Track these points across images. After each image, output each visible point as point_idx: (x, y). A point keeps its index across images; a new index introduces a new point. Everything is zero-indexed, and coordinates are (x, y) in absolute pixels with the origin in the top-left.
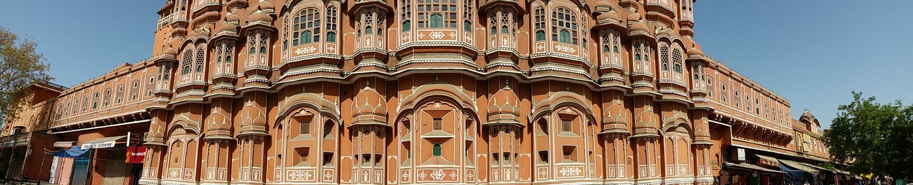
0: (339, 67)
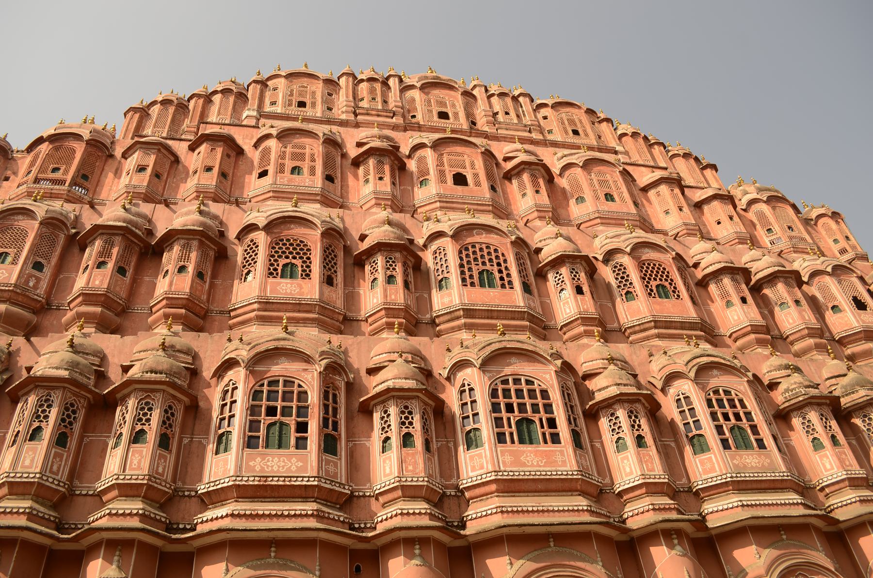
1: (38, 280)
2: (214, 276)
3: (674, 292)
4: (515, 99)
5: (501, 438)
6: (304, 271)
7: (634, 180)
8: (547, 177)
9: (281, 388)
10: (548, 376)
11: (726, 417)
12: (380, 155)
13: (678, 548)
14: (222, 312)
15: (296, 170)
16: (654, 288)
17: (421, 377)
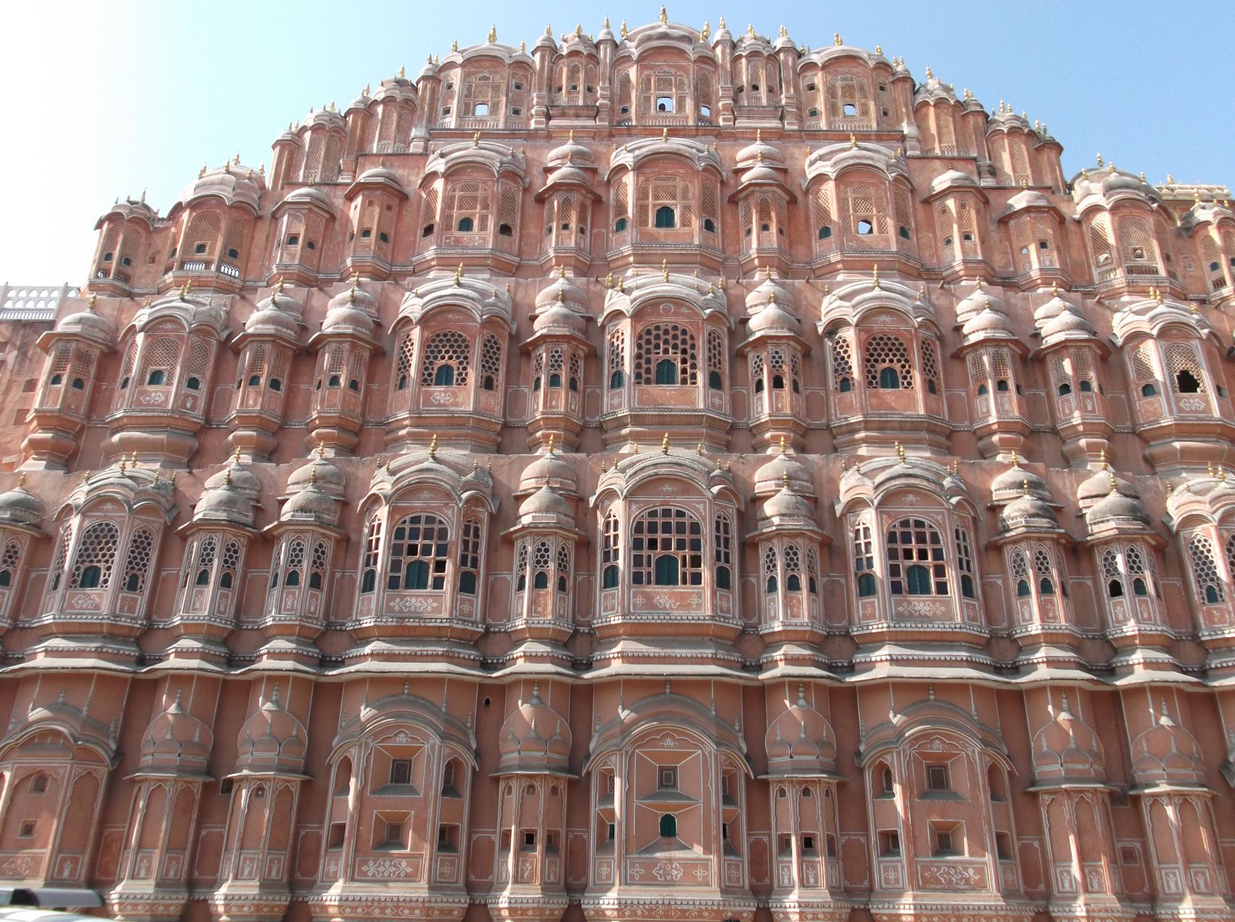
0: (475, 646)
1: (195, 398)
2: (370, 379)
3: (905, 378)
4: (773, 57)
5: (637, 579)
6: (460, 374)
7: (913, 191)
8: (787, 198)
9: (422, 526)
10: (701, 507)
12: (567, 191)
13: (802, 702)
14: (379, 424)
15: (466, 224)
16: (878, 375)
17: (567, 508)
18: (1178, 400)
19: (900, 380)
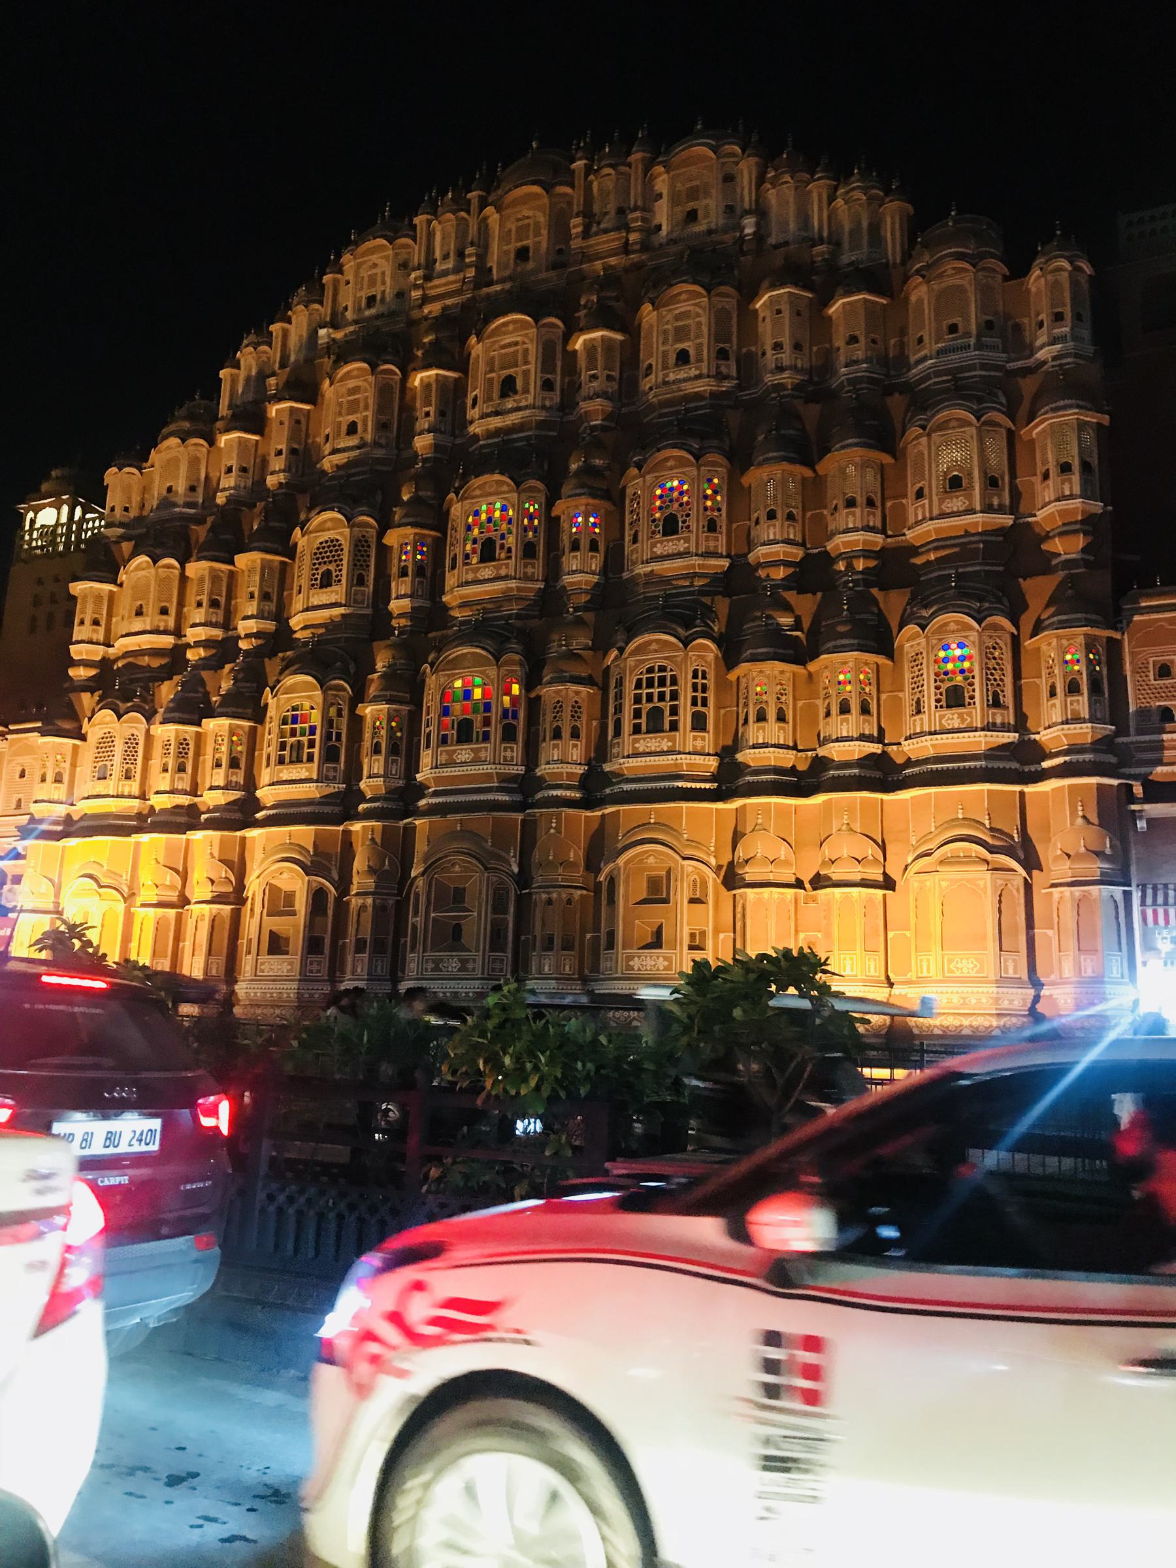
1: (166, 621)
11: (650, 698)
15: (352, 429)
18: (941, 501)
19: (680, 524)
